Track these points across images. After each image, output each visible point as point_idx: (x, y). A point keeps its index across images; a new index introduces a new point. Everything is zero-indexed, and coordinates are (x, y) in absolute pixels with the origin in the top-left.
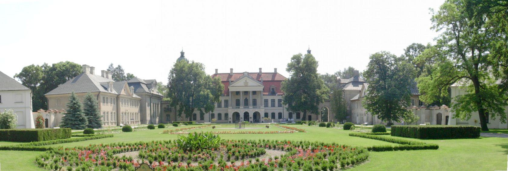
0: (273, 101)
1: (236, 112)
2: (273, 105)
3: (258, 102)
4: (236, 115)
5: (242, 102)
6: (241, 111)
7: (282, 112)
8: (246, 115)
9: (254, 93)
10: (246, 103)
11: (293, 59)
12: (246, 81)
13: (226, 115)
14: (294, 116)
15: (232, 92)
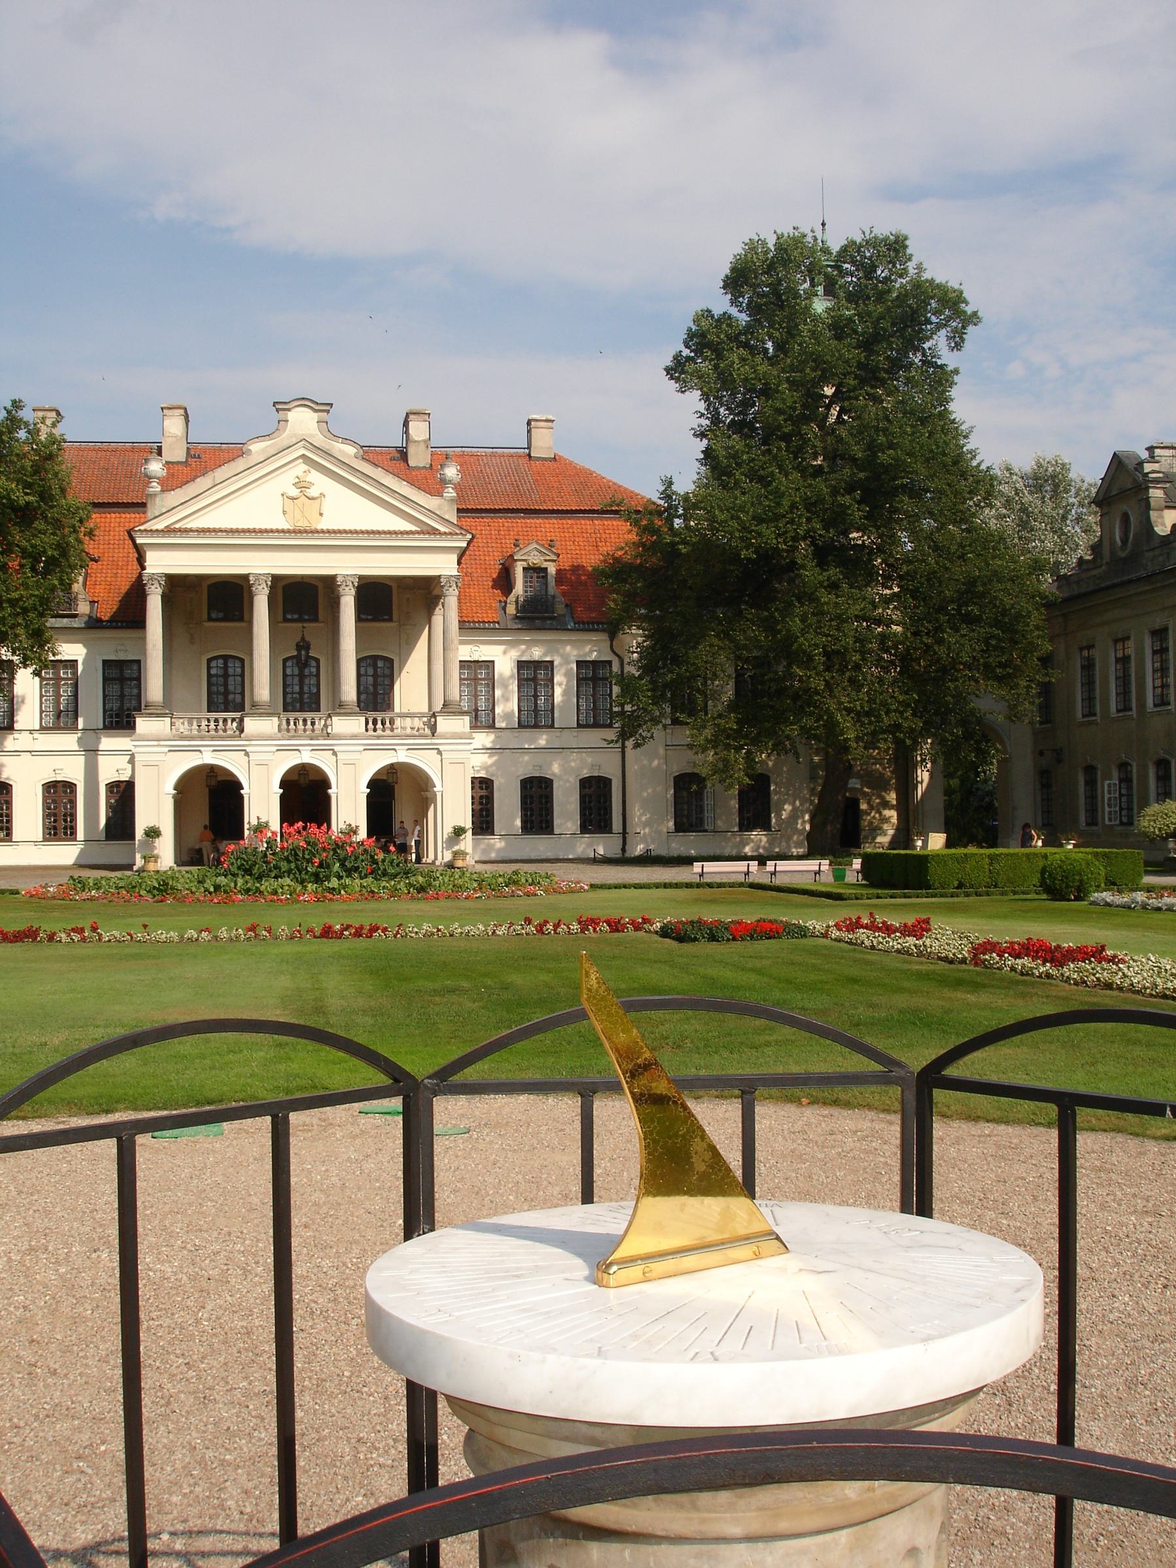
0: (533, 675)
1: (211, 772)
2: (536, 716)
3: (411, 689)
4: (213, 800)
5: (263, 679)
6: (260, 763)
7: (608, 767)
8: (306, 795)
9: (378, 598)
10: (302, 695)
11: (738, 280)
12: (301, 485)
13: (123, 796)
14: (726, 804)
15: (178, 587)
